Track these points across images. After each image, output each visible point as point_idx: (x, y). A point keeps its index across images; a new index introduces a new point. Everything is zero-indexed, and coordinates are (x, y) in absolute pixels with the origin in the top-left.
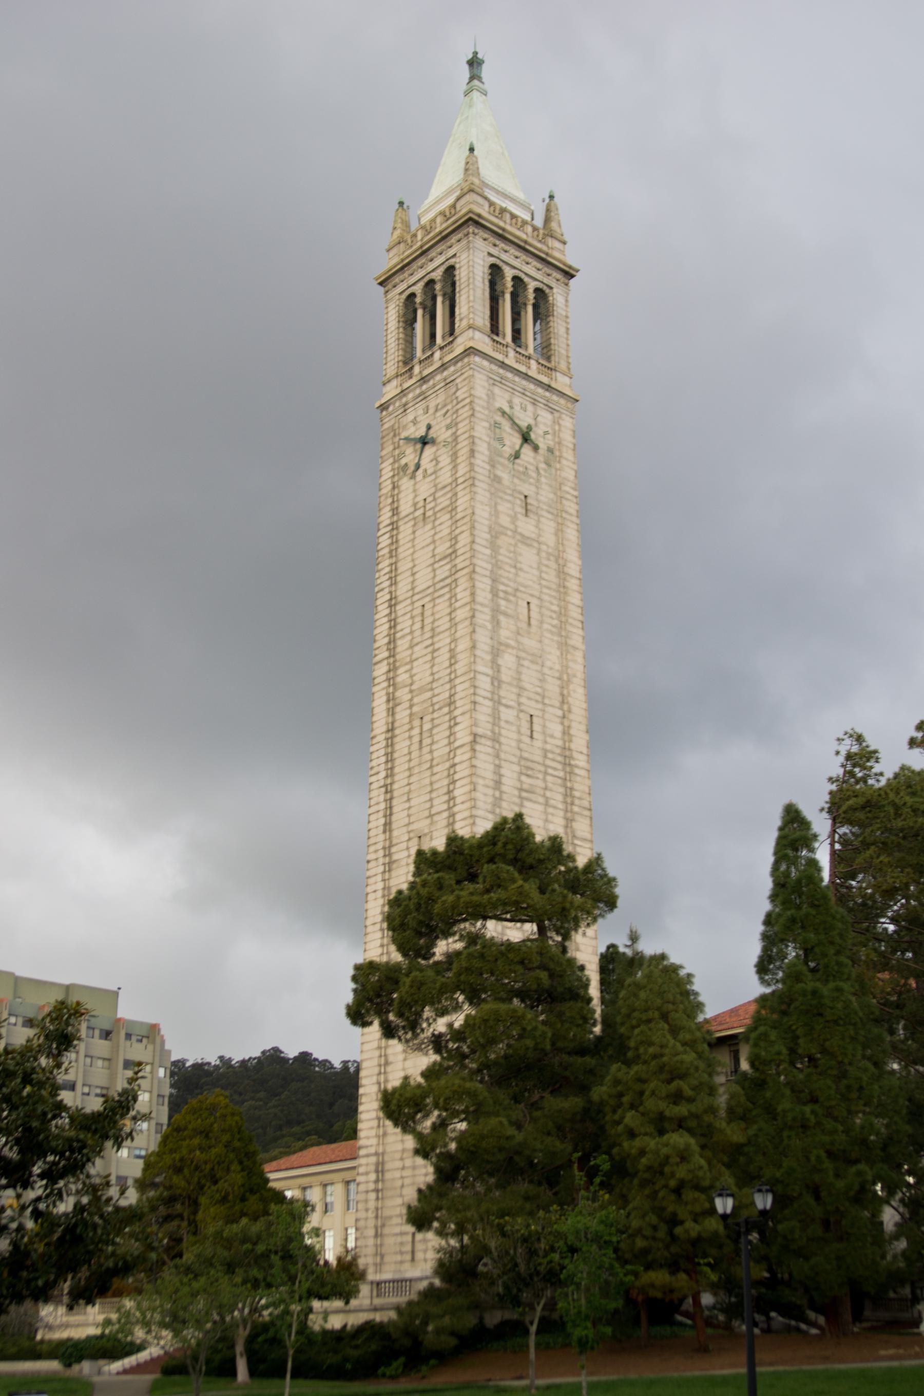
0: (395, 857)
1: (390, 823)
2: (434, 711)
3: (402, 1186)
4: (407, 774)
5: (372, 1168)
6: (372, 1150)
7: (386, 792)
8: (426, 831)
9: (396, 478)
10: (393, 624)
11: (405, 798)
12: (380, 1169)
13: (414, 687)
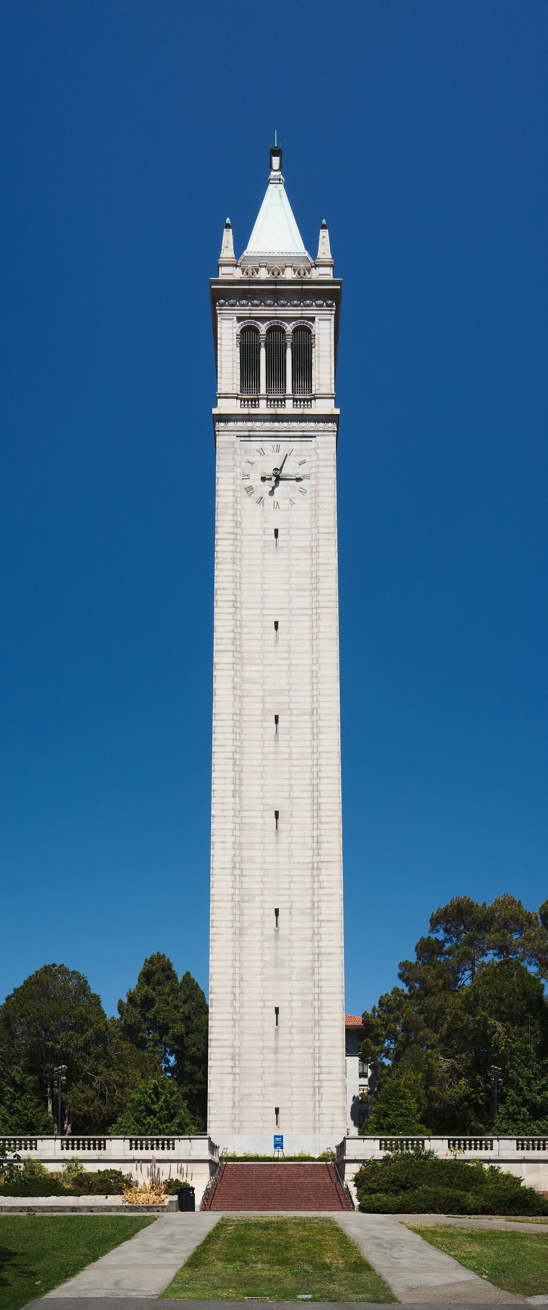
0: (245, 821)
1: (240, 791)
2: (291, 715)
3: (264, 1073)
4: (261, 757)
5: (230, 1056)
6: (229, 1043)
7: (235, 764)
8: (285, 808)
9: (238, 494)
10: (238, 625)
11: (259, 775)
12: (236, 1058)
13: (266, 687)
